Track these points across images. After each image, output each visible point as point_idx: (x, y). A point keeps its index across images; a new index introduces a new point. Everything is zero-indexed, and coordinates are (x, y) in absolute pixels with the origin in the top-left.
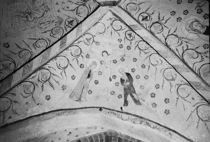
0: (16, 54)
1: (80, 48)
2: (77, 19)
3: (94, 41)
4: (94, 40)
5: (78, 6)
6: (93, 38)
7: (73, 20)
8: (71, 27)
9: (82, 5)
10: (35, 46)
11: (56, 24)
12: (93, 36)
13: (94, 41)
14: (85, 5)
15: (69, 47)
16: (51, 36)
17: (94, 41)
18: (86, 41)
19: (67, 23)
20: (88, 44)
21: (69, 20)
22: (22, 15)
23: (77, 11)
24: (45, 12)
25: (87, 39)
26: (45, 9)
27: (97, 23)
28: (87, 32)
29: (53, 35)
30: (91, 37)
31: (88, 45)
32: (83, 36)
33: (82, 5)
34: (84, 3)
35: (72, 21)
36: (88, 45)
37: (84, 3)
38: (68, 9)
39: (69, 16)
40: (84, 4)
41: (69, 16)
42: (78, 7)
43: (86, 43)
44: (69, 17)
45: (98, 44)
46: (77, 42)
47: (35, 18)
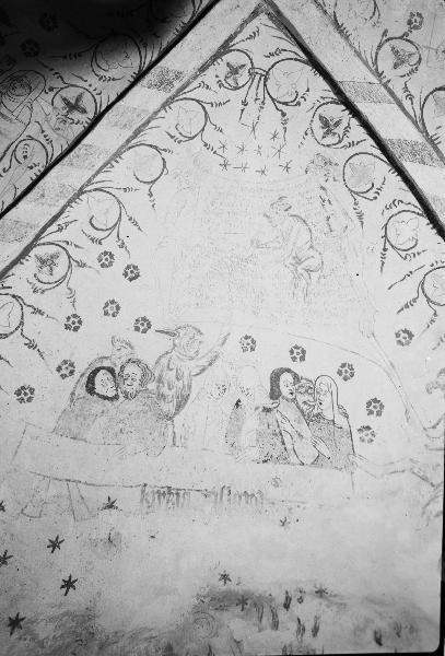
0: (435, 314)
1: (432, 93)
2: (318, 104)
3: (404, 37)
5: (268, 100)
6: (391, 39)
7: (321, 117)
8: (349, 126)
9: (265, 85)
10: (409, 252)
11: (331, 179)
12: (385, 38)
13: (406, 34)
14: (267, 73)
16: (376, 198)
17: (404, 37)
18: (405, 69)
19: (330, 140)
20: (414, 60)
21: (319, 132)
22: (303, 283)
23: (286, 104)
24: (291, 212)
25: (396, 66)
26: (282, 212)
29: (374, 190)
30: (387, 47)
31: (420, 59)
32: (384, 81)
33: (265, 85)
34: (258, 77)
35: (325, 123)
36: (420, 59)
37: (258, 77)
38: (281, 135)
39: (306, 134)
40: (262, 75)
41: (306, 134)
42: (273, 99)
43: (410, 68)
44: (309, 132)
45: (418, 19)
46: (407, 104)
47: (311, 247)
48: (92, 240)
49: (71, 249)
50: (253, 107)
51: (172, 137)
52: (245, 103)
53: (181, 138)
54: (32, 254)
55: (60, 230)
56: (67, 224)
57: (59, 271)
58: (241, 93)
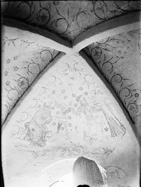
4: (94, 5)
6: (94, 9)
15: (129, 11)
27: (86, 28)
28: (101, 21)
30: (96, 11)
34: (99, 46)
37: (99, 46)
38: (118, 41)
40: (99, 45)
42: (107, 42)
43: (105, 6)
48: (131, 97)
49: (131, 102)
50: (108, 47)
51: (111, 72)
52: (106, 49)
53: (112, 70)
54: (128, 110)
55: (126, 103)
56: (125, 101)
57: (134, 106)
58: (103, 51)
